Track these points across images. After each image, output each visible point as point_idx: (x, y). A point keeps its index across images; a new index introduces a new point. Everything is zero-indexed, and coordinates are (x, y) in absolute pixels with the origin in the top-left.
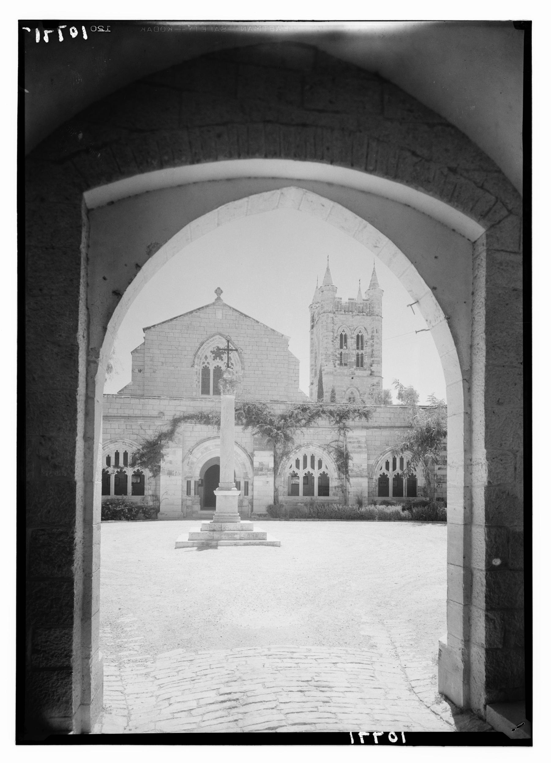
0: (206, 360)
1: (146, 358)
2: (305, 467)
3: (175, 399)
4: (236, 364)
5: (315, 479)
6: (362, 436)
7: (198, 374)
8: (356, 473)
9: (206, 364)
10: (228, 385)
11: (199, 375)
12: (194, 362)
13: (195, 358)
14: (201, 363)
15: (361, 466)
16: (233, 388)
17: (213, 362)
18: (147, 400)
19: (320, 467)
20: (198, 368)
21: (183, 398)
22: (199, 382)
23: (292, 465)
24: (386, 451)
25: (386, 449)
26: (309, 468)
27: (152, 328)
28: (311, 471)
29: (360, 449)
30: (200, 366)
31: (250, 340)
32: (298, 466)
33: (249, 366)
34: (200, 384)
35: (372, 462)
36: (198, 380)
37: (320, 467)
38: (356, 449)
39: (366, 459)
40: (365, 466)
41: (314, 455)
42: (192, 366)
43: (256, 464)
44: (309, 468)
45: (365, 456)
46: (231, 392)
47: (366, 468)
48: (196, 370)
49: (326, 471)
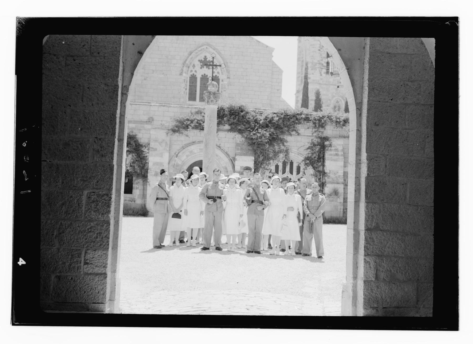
0: (194, 68)
2: (284, 172)
3: (164, 106)
4: (222, 72)
6: (339, 145)
7: (186, 81)
8: (333, 179)
9: (194, 72)
10: (212, 96)
11: (187, 82)
12: (182, 70)
13: (183, 67)
14: (189, 71)
15: (338, 172)
16: (216, 99)
17: (201, 70)
18: (138, 106)
20: (187, 76)
21: (171, 104)
22: (186, 89)
29: (337, 157)
30: (188, 74)
33: (234, 75)
34: (188, 91)
36: (186, 88)
38: (333, 157)
39: (343, 167)
41: (293, 161)
42: (181, 74)
46: (215, 102)
47: (342, 174)
48: (184, 78)
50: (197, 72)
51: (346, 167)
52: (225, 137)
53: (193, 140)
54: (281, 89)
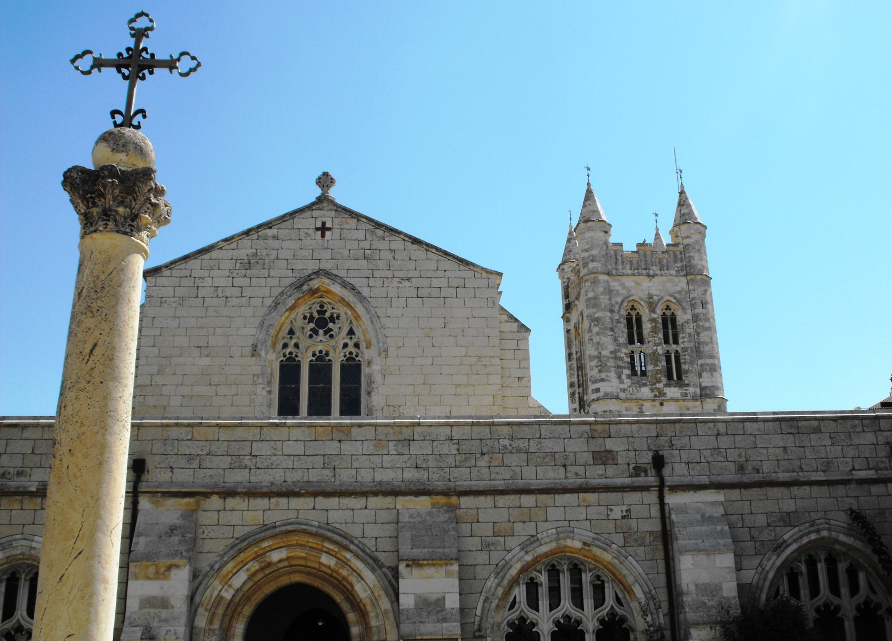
2: (555, 603)
5: (587, 636)
17: (309, 341)
19: (599, 601)
20: (273, 360)
22: (270, 392)
23: (517, 600)
24: (785, 541)
25: (786, 537)
26: (566, 605)
28: (575, 613)
32: (533, 604)
35: (750, 575)
37: (599, 601)
40: (730, 590)
43: (407, 601)
44: (566, 605)
45: (727, 560)
50: (300, 346)
51: (741, 569)
52: (366, 508)
53: (266, 522)
54: (529, 377)
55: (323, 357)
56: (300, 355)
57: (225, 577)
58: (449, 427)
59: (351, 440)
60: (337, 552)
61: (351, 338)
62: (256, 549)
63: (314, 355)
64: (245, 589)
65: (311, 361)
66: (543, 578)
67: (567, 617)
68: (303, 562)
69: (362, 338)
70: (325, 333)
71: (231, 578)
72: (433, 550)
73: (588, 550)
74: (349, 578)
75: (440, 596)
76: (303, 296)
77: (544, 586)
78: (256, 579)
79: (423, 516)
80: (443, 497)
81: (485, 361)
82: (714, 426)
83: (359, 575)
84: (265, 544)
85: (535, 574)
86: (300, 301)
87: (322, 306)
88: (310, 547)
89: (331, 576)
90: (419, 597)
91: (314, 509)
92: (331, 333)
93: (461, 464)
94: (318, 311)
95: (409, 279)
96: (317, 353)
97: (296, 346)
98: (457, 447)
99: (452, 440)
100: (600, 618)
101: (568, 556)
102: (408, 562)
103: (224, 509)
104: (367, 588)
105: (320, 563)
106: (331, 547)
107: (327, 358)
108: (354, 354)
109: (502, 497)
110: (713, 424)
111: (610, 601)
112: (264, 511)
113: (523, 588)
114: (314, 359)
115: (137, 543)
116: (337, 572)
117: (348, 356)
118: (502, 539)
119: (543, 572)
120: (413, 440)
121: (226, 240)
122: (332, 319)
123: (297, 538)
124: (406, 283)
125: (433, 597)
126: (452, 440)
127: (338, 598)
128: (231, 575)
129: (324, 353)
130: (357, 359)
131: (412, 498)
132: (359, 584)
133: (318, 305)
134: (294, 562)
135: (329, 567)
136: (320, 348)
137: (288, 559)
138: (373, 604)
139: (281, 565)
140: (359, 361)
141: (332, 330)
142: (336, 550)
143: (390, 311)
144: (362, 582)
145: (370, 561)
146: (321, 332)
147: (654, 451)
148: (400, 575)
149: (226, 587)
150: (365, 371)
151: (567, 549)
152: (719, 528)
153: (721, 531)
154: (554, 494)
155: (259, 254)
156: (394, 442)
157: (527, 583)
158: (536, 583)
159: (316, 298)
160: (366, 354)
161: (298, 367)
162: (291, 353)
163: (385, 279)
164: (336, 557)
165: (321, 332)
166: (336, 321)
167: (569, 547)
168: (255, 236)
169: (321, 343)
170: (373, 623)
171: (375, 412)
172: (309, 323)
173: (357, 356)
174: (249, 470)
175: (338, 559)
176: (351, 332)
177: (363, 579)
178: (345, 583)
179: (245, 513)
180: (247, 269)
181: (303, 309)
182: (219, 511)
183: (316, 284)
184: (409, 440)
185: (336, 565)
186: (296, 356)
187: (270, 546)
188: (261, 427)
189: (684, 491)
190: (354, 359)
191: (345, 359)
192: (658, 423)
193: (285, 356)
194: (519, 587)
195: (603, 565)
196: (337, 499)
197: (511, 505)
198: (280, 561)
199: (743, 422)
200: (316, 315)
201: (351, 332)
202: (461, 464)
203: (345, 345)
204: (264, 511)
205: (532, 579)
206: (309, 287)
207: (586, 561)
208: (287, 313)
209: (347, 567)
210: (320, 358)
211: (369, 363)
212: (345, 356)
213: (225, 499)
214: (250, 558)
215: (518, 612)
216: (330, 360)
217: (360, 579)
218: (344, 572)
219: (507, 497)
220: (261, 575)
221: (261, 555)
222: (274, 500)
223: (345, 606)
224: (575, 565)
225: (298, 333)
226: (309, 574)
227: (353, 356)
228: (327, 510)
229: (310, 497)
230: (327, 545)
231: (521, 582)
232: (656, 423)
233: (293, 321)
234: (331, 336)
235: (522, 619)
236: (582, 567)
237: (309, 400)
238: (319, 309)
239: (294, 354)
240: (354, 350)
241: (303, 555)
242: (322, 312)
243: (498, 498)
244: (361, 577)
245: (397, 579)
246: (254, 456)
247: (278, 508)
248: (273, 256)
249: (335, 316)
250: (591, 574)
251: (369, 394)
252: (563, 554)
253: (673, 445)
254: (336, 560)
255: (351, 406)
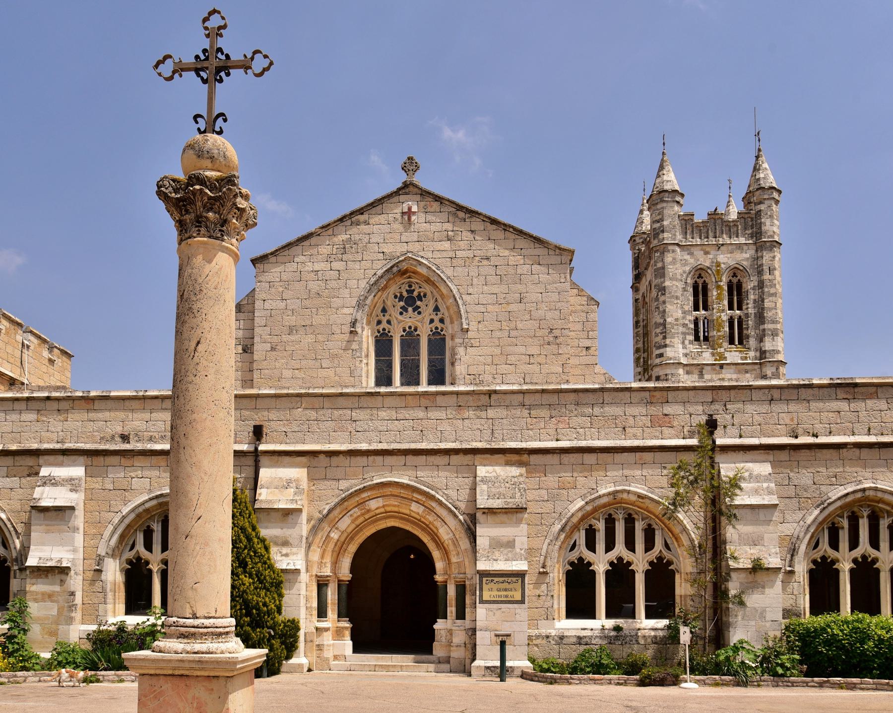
1: (257, 320)
2: (610, 546)
5: (637, 576)
9: (384, 325)
19: (649, 545)
26: (620, 549)
27: (270, 256)
28: (627, 555)
31: (480, 264)
32: (591, 545)
37: (649, 545)
44: (620, 549)
49: (667, 555)
52: (449, 464)
55: (412, 332)
56: (392, 331)
57: (332, 521)
58: (522, 394)
59: (436, 407)
60: (424, 502)
61: (437, 314)
62: (357, 499)
63: (404, 330)
64: (349, 530)
65: (402, 336)
66: (601, 526)
67: (620, 559)
68: (396, 509)
69: (446, 314)
70: (414, 311)
71: (337, 522)
72: (506, 500)
73: (642, 502)
74: (434, 523)
75: (511, 539)
76: (394, 277)
77: (601, 531)
78: (358, 522)
79: (498, 472)
80: (515, 455)
81: (557, 333)
82: (769, 391)
83: (443, 520)
84: (365, 495)
85: (594, 522)
86: (391, 282)
87: (410, 286)
88: (402, 497)
89: (420, 520)
90: (494, 539)
91: (405, 465)
92: (419, 310)
93: (531, 427)
94: (407, 291)
95: (488, 259)
96: (407, 329)
97: (389, 322)
98: (528, 412)
99: (524, 405)
100: (649, 561)
101: (623, 507)
102: (484, 510)
103: (330, 466)
104: (450, 531)
105: (410, 510)
106: (420, 497)
107: (416, 333)
108: (440, 329)
109: (567, 455)
110: (768, 390)
111: (659, 545)
112: (363, 467)
113: (583, 533)
114: (404, 334)
115: (260, 494)
116: (424, 518)
117: (434, 331)
118: (564, 492)
119: (601, 520)
120: (490, 406)
121: (323, 227)
122: (420, 298)
123: (390, 490)
124: (485, 262)
125: (505, 540)
126: (524, 405)
127: (425, 539)
128: (337, 519)
129: (413, 328)
130: (442, 333)
131: (488, 456)
132: (443, 528)
133: (407, 285)
134: (388, 509)
135: (418, 514)
136: (410, 324)
137: (384, 506)
138: (455, 544)
139: (378, 511)
140: (444, 335)
141: (420, 307)
142: (424, 499)
143: (471, 290)
144: (446, 526)
145: (453, 509)
146: (410, 309)
147: (708, 415)
148: (477, 521)
149: (334, 529)
150: (449, 343)
151: (623, 501)
152: (765, 485)
153: (768, 487)
154: (614, 453)
155: (353, 239)
156: (474, 408)
157: (586, 530)
158: (594, 529)
159: (405, 278)
160: (449, 329)
161: (390, 342)
162: (384, 329)
163: (467, 259)
164: (423, 505)
165: (410, 309)
166: (423, 299)
167: (625, 499)
168: (349, 222)
169: (410, 319)
170: (454, 559)
171: (458, 380)
172: (399, 301)
173: (442, 330)
174: (349, 433)
175: (425, 507)
176: (437, 309)
177: (446, 524)
178: (431, 526)
179: (348, 469)
180: (342, 254)
181: (393, 289)
182: (326, 468)
183: (404, 266)
184: (487, 406)
185: (423, 512)
186: (389, 332)
187: (368, 496)
188: (359, 396)
189: (734, 451)
190: (439, 334)
191: (431, 333)
192: (714, 390)
193: (379, 332)
194: (580, 532)
195: (654, 515)
196: (425, 457)
197: (575, 463)
198: (377, 509)
199: (798, 388)
200: (405, 294)
201: (437, 309)
202: (531, 427)
203: (432, 321)
204: (363, 467)
205: (591, 526)
206: (398, 269)
207: (639, 511)
208: (380, 293)
209: (433, 513)
210: (410, 334)
211: (452, 338)
212: (431, 331)
213: (330, 457)
214: (353, 506)
215: (578, 553)
216: (418, 335)
217: (443, 524)
218: (431, 518)
219: (571, 455)
220: (361, 519)
221: (361, 503)
222: (371, 458)
223: (431, 546)
224: (630, 515)
225: (391, 310)
226: (402, 518)
227: (439, 331)
228: (416, 466)
229: (401, 455)
230: (415, 495)
231: (581, 528)
232: (713, 390)
233: (386, 300)
234: (419, 313)
235: (581, 559)
236: (635, 516)
237: (401, 370)
238: (408, 289)
239: (387, 330)
240: (439, 325)
241: (396, 503)
242: (410, 292)
243: (563, 456)
244: (445, 522)
245: (475, 525)
246: (354, 421)
247: (374, 465)
248: (366, 240)
249: (422, 294)
250: (643, 522)
251: (453, 364)
252: (620, 505)
253: (727, 409)
254: (424, 507)
255: (437, 377)
